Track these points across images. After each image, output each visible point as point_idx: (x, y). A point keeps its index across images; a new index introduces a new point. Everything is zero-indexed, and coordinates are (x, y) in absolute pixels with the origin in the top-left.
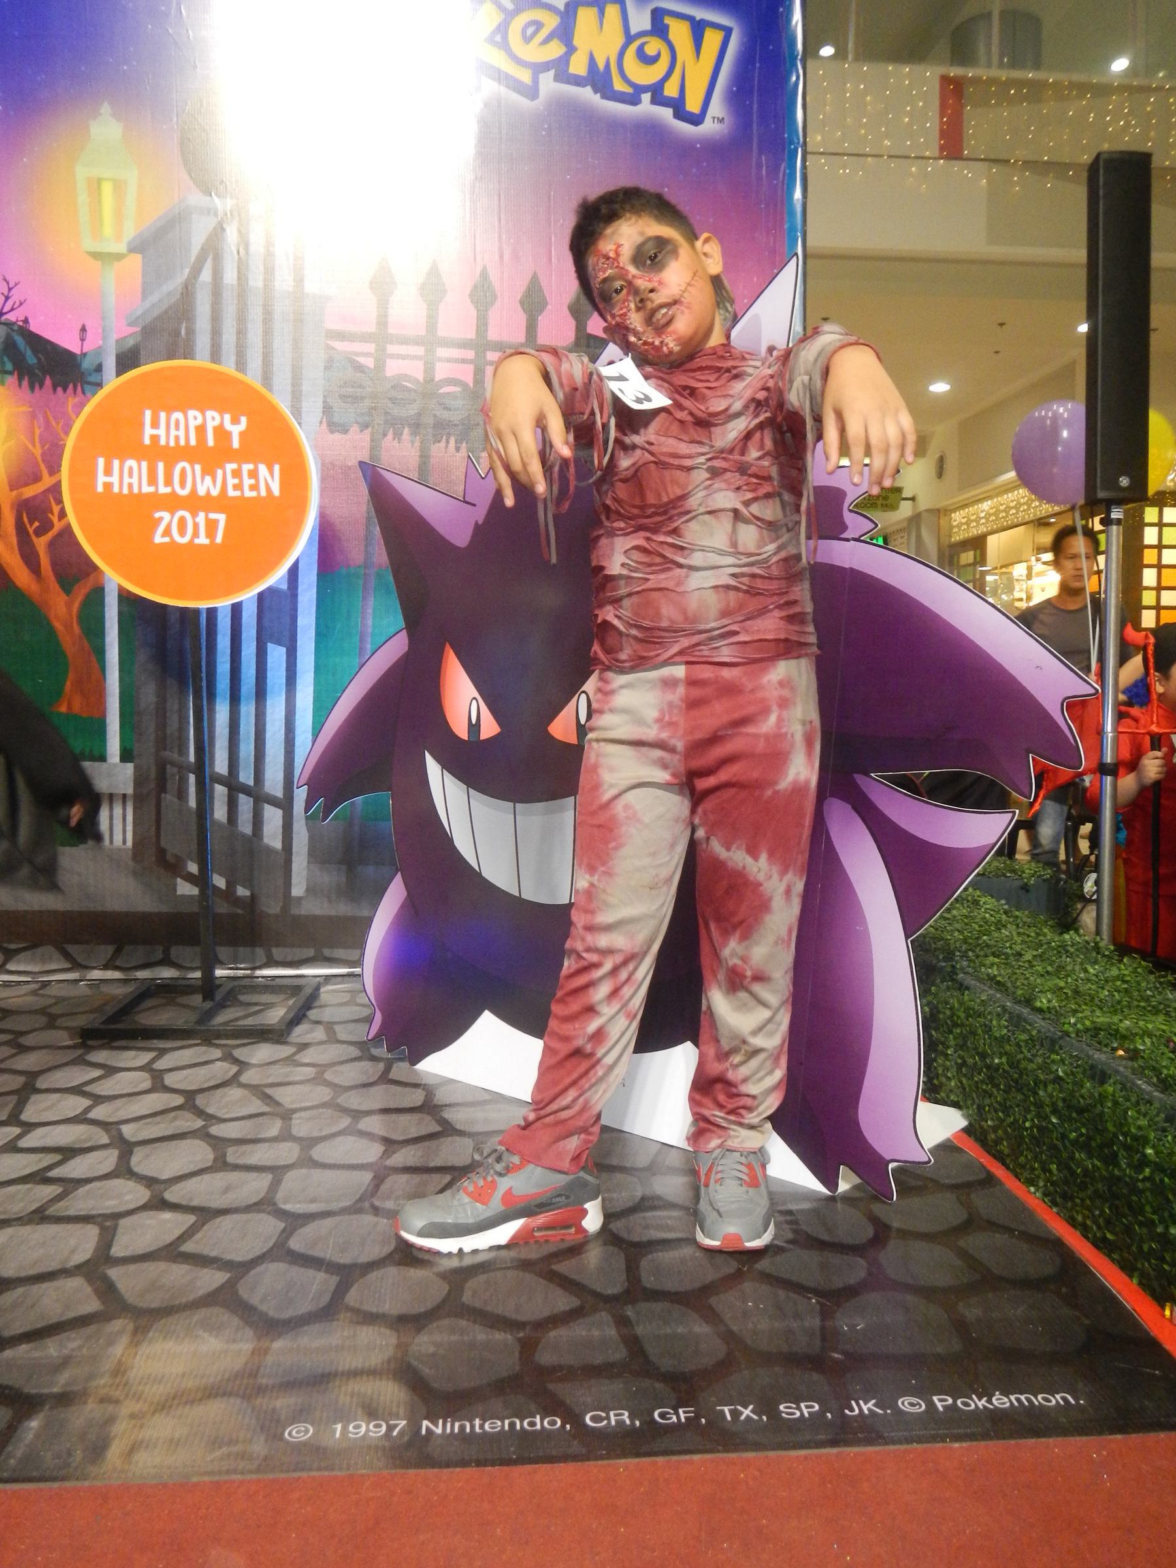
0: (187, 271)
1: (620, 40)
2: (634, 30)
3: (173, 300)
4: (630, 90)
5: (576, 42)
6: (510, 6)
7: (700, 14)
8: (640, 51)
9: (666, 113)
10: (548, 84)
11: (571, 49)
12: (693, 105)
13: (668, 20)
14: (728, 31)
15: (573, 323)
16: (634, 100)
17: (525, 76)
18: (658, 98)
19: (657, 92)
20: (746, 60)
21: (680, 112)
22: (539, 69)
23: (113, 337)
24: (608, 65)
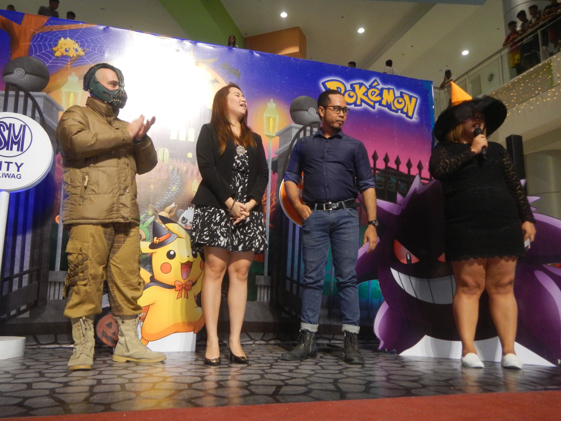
0: (291, 142)
1: (393, 98)
2: (396, 96)
3: (286, 149)
5: (383, 97)
6: (368, 87)
7: (411, 94)
9: (404, 116)
10: (377, 105)
11: (382, 99)
12: (410, 114)
13: (404, 95)
14: (417, 99)
16: (397, 112)
17: (372, 104)
19: (402, 110)
21: (407, 116)
22: (375, 102)
23: (271, 157)
24: (391, 102)
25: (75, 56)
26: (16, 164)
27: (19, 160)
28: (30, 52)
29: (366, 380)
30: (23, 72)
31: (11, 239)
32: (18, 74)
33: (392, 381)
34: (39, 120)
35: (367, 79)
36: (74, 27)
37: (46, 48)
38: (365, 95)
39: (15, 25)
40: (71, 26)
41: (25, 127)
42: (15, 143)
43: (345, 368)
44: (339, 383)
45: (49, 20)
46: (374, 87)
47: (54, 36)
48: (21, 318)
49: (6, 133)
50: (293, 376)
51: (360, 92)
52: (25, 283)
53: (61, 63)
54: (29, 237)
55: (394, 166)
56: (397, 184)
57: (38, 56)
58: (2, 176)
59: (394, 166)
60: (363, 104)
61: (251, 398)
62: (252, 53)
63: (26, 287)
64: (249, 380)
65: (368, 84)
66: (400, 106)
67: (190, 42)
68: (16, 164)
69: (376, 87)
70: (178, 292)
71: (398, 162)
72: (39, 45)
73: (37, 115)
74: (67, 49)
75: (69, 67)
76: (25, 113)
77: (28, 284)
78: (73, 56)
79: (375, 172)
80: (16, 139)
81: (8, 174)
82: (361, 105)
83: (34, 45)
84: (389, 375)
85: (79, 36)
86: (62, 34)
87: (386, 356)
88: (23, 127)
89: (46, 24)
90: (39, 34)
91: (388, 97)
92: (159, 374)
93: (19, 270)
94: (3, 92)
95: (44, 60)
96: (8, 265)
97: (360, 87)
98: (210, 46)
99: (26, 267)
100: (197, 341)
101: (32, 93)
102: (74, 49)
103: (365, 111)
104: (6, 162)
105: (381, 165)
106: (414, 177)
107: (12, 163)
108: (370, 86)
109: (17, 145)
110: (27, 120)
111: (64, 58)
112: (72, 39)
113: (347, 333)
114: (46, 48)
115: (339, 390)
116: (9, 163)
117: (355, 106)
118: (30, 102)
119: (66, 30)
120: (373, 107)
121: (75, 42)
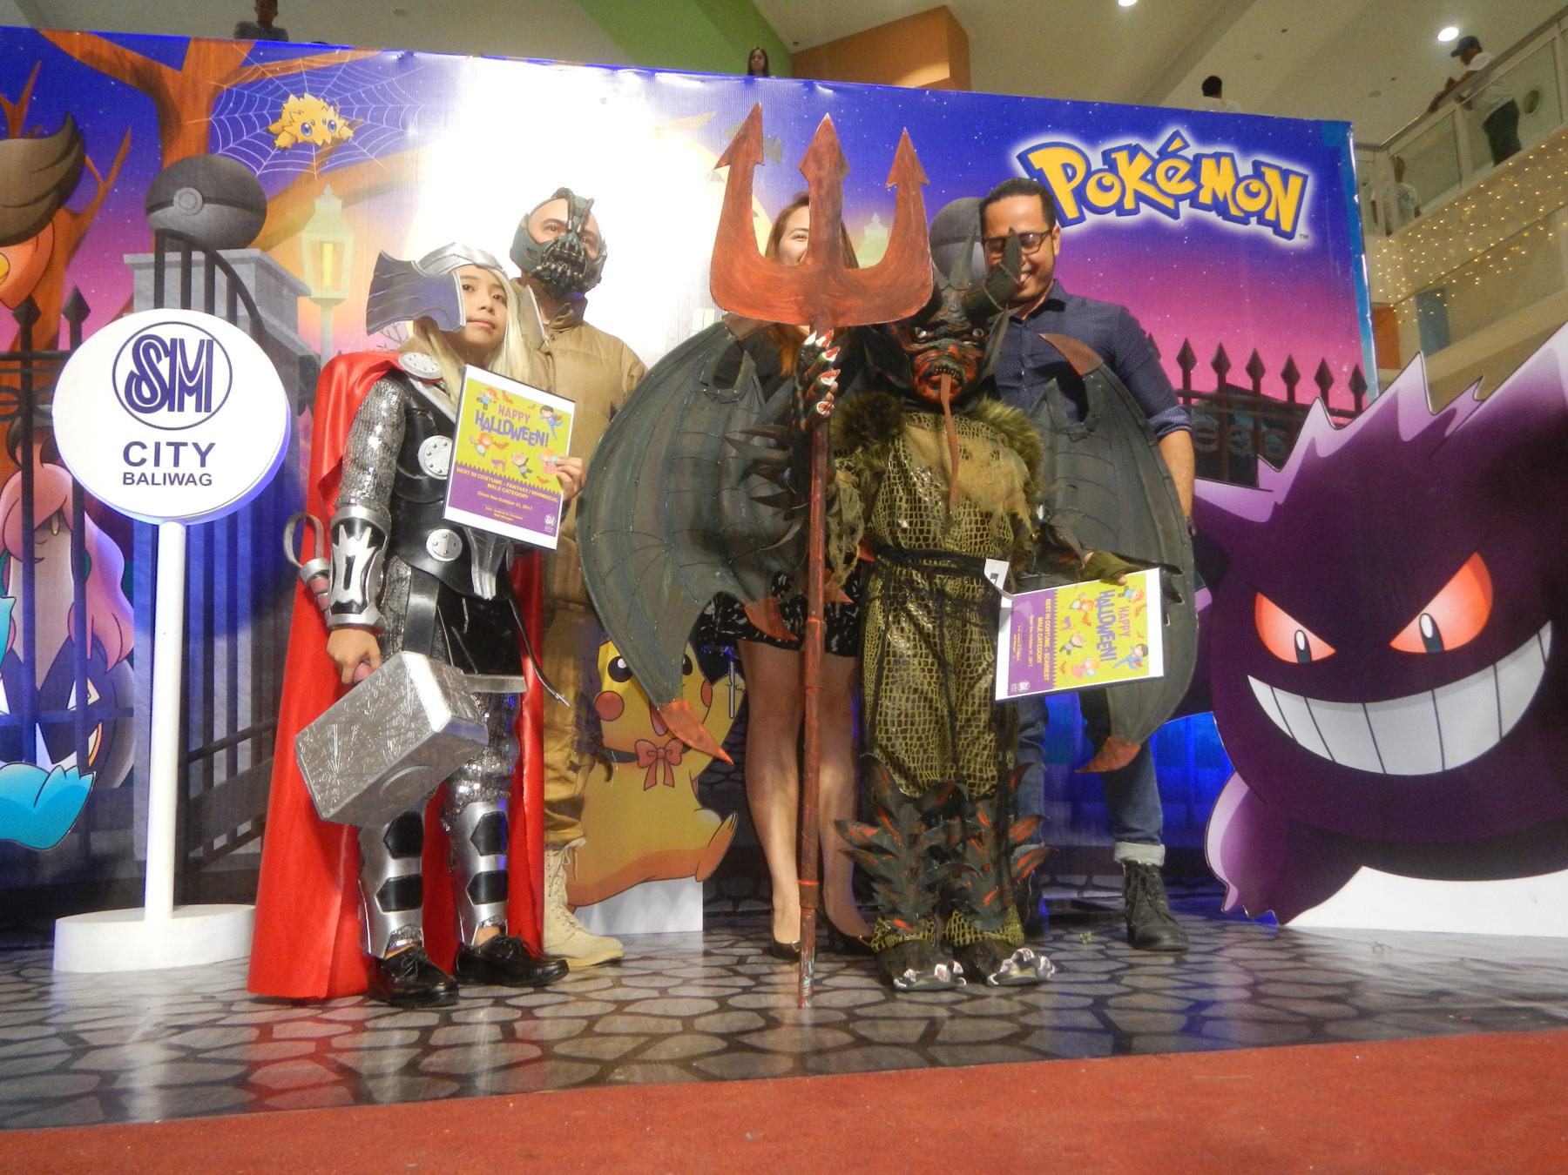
1: (1232, 182)
2: (1241, 175)
4: (1242, 215)
5: (1202, 181)
6: (1156, 157)
7: (1286, 165)
8: (1247, 187)
9: (1268, 231)
10: (1185, 208)
11: (1200, 186)
12: (1286, 226)
13: (1263, 169)
14: (1305, 178)
15: (1214, 376)
16: (1245, 221)
17: (1169, 203)
18: (1262, 221)
19: (1260, 216)
20: (1319, 197)
22: (1178, 199)
24: (1225, 194)
25: (329, 141)
26: (196, 446)
27: (202, 436)
28: (211, 143)
29: (1188, 999)
30: (196, 197)
31: (197, 647)
32: (184, 205)
33: (1265, 1001)
34: (248, 326)
35: (1150, 132)
36: (318, 63)
37: (251, 128)
38: (1148, 181)
39: (166, 71)
40: (312, 61)
41: (210, 344)
42: (190, 391)
43: (1126, 965)
44: (1108, 1007)
45: (253, 50)
46: (1174, 155)
47: (271, 93)
48: (242, 855)
49: (164, 367)
50: (976, 992)
51: (1132, 172)
52: (244, 763)
53: (294, 165)
54: (245, 639)
55: (1246, 383)
56: (1255, 433)
57: (231, 150)
58: (162, 482)
59: (1246, 383)
60: (1143, 206)
61: (857, 1054)
62: (812, 89)
63: (248, 774)
64: (851, 1004)
65: (1153, 148)
66: (1253, 205)
67: (636, 73)
68: (196, 446)
69: (1180, 153)
70: (646, 770)
71: (1255, 369)
72: (234, 122)
73: (242, 311)
74: (307, 126)
75: (315, 173)
76: (210, 308)
77: (252, 764)
78: (324, 142)
79: (1187, 401)
80: (191, 381)
81: (177, 475)
82: (1136, 211)
83: (220, 122)
84: (1257, 983)
85: (335, 85)
86: (292, 84)
87: (1248, 929)
88: (207, 347)
89: (247, 63)
90: (228, 90)
91: (1217, 180)
92: (605, 995)
93: (225, 728)
94: (151, 257)
95: (253, 163)
96: (197, 717)
97: (1132, 158)
98: (691, 79)
99: (245, 720)
100: (706, 904)
101: (223, 253)
102: (324, 122)
103: (1151, 227)
104: (169, 444)
105: (1204, 380)
106: (1306, 409)
107: (185, 444)
108: (1159, 153)
109: (194, 396)
110: (217, 325)
111: (301, 149)
112: (317, 97)
113: (1132, 865)
114: (251, 128)
115: (1109, 1027)
116: (177, 446)
117: (1119, 214)
118: (221, 278)
119: (300, 74)
120: (1174, 214)
121: (327, 106)
